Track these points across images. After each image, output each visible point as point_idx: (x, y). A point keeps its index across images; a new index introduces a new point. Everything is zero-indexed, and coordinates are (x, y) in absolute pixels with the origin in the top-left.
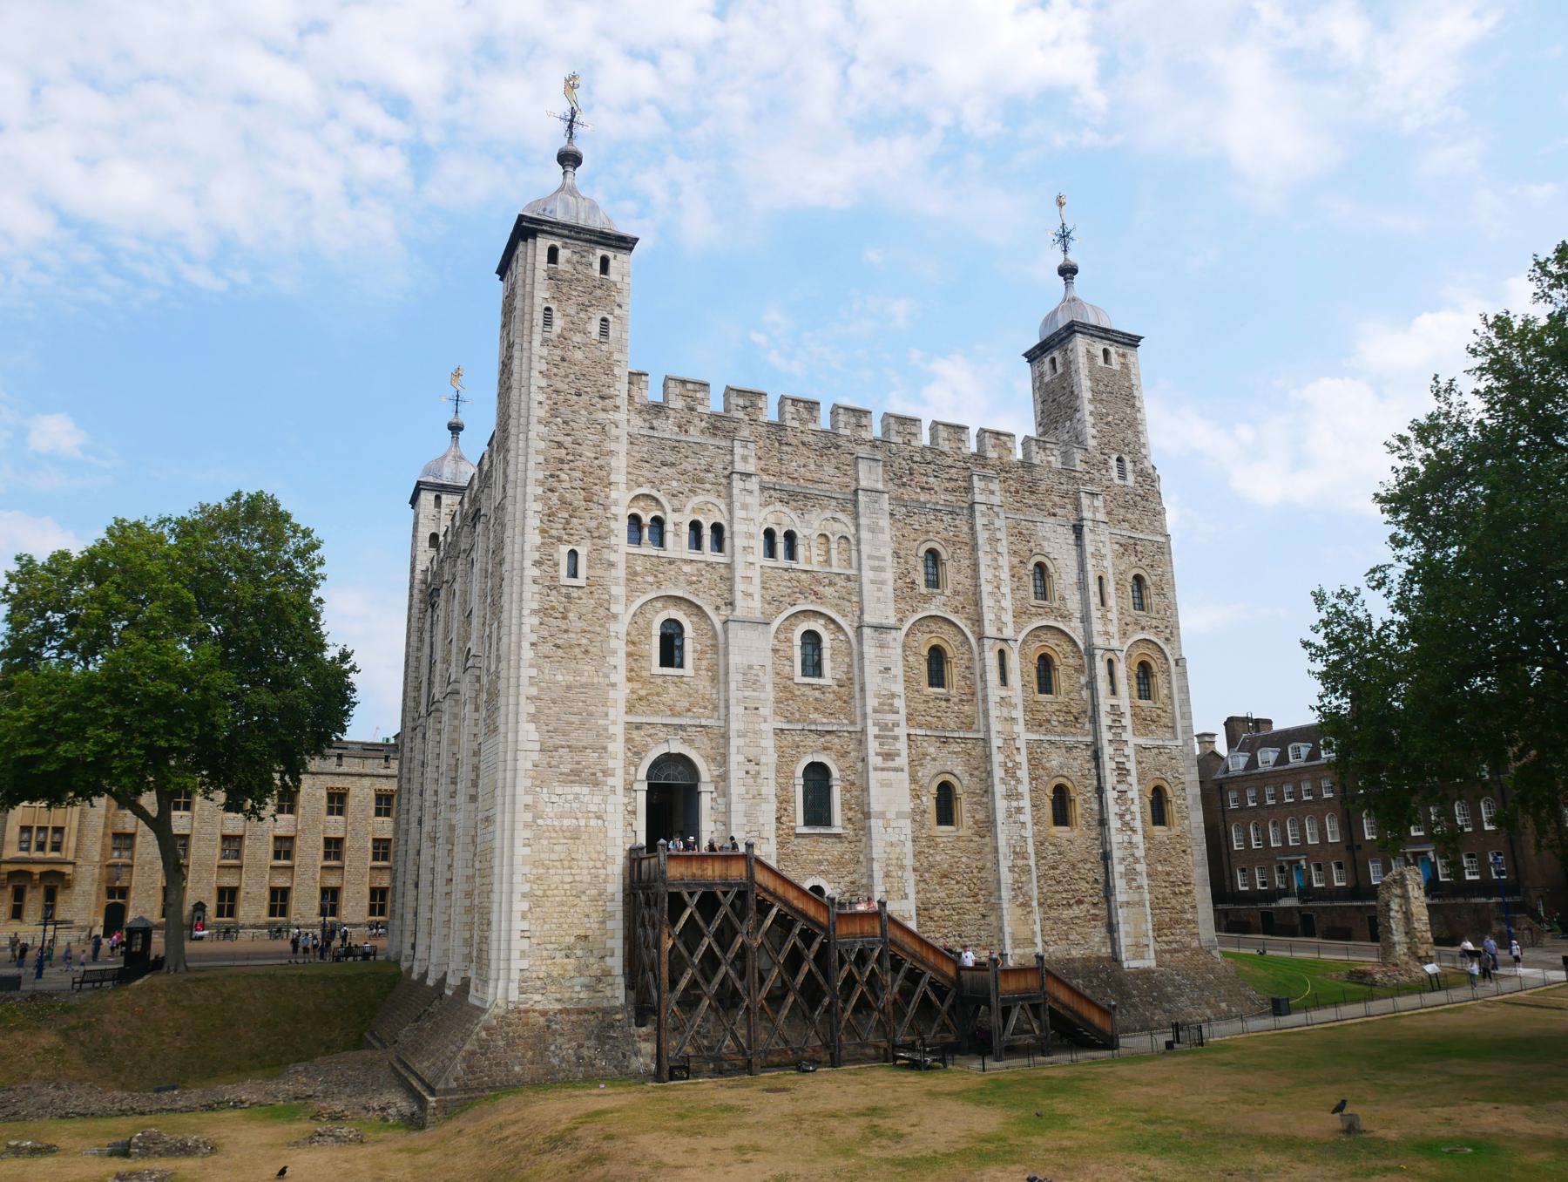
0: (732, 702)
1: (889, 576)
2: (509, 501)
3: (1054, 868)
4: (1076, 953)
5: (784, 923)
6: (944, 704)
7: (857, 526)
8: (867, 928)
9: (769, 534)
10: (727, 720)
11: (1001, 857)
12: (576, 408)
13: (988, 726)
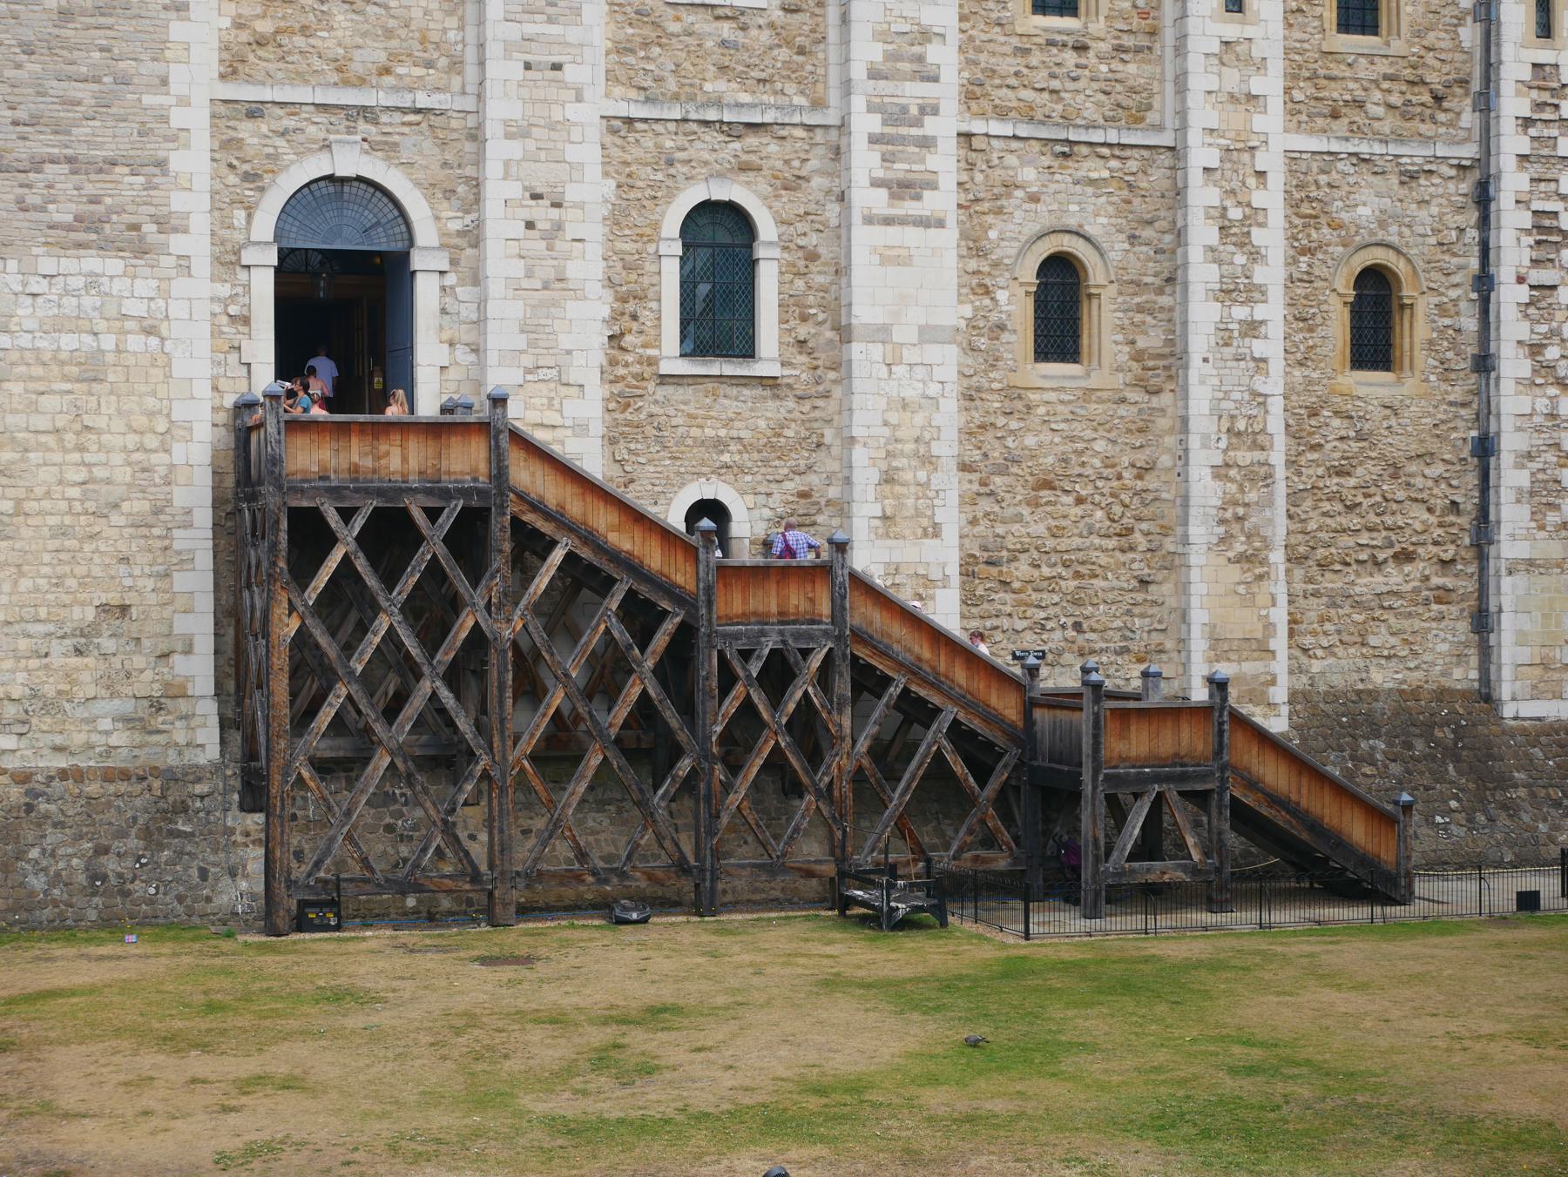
0: (493, 50)
3: (1341, 473)
4: (1381, 677)
5: (583, 578)
6: (1070, 57)
8: (796, 599)
10: (480, 97)
11: (1194, 442)
13: (1182, 114)
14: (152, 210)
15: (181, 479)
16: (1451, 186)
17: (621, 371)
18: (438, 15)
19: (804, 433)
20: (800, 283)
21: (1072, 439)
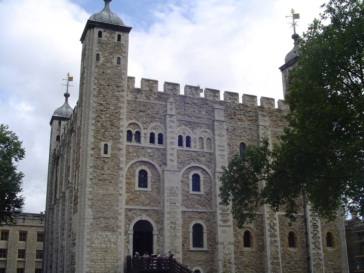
0: (166, 201)
1: (226, 153)
2: (82, 126)
3: (288, 263)
7: (214, 134)
9: (180, 137)
12: (107, 91)
14: (116, 225)
15: (119, 267)
16: (301, 219)
17: (184, 250)
18: (157, 196)
19: (211, 259)
20: (210, 236)
21: (250, 259)
